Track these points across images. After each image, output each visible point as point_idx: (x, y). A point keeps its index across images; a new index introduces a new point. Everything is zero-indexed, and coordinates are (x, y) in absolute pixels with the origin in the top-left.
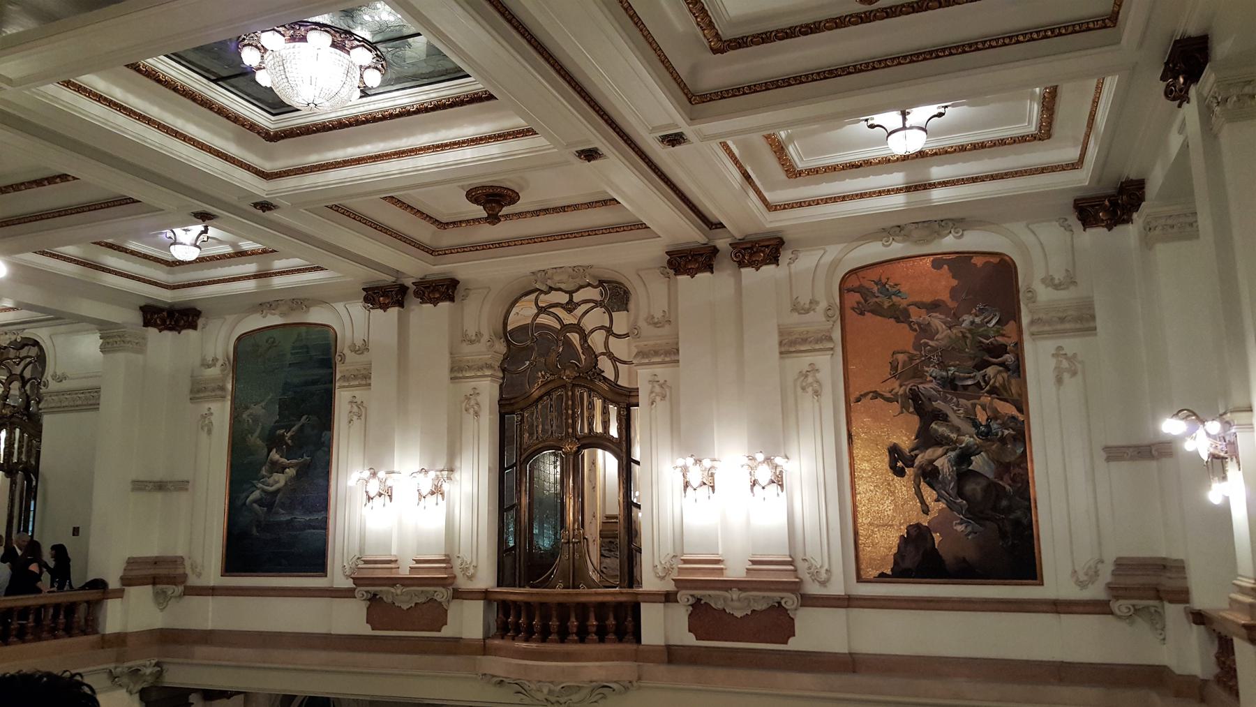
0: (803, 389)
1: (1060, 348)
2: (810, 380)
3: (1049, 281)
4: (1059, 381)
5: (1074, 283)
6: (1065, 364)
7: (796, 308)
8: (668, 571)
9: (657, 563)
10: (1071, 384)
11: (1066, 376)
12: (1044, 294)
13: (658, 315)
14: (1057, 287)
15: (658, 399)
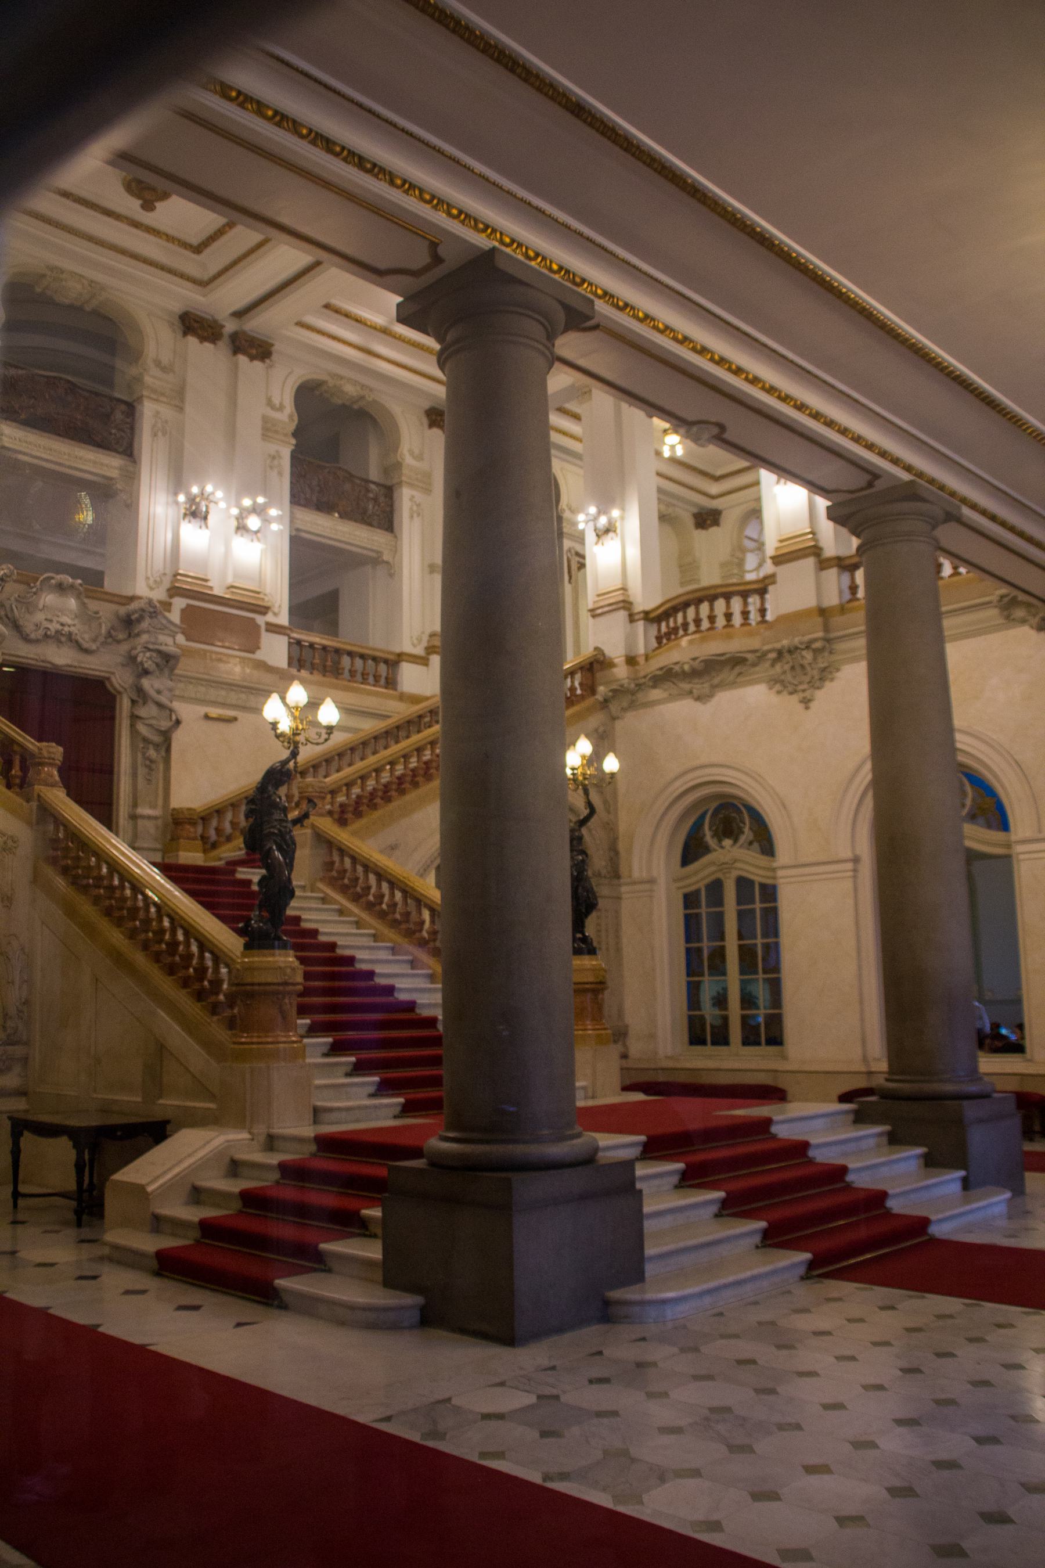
0: (271, 467)
1: (413, 497)
2: (276, 462)
3: (411, 452)
4: (412, 517)
5: (422, 459)
6: (415, 508)
7: (270, 403)
8: (158, 583)
9: (149, 575)
10: (417, 521)
11: (415, 515)
12: (409, 460)
13: (165, 360)
14: (415, 458)
15: (160, 434)
